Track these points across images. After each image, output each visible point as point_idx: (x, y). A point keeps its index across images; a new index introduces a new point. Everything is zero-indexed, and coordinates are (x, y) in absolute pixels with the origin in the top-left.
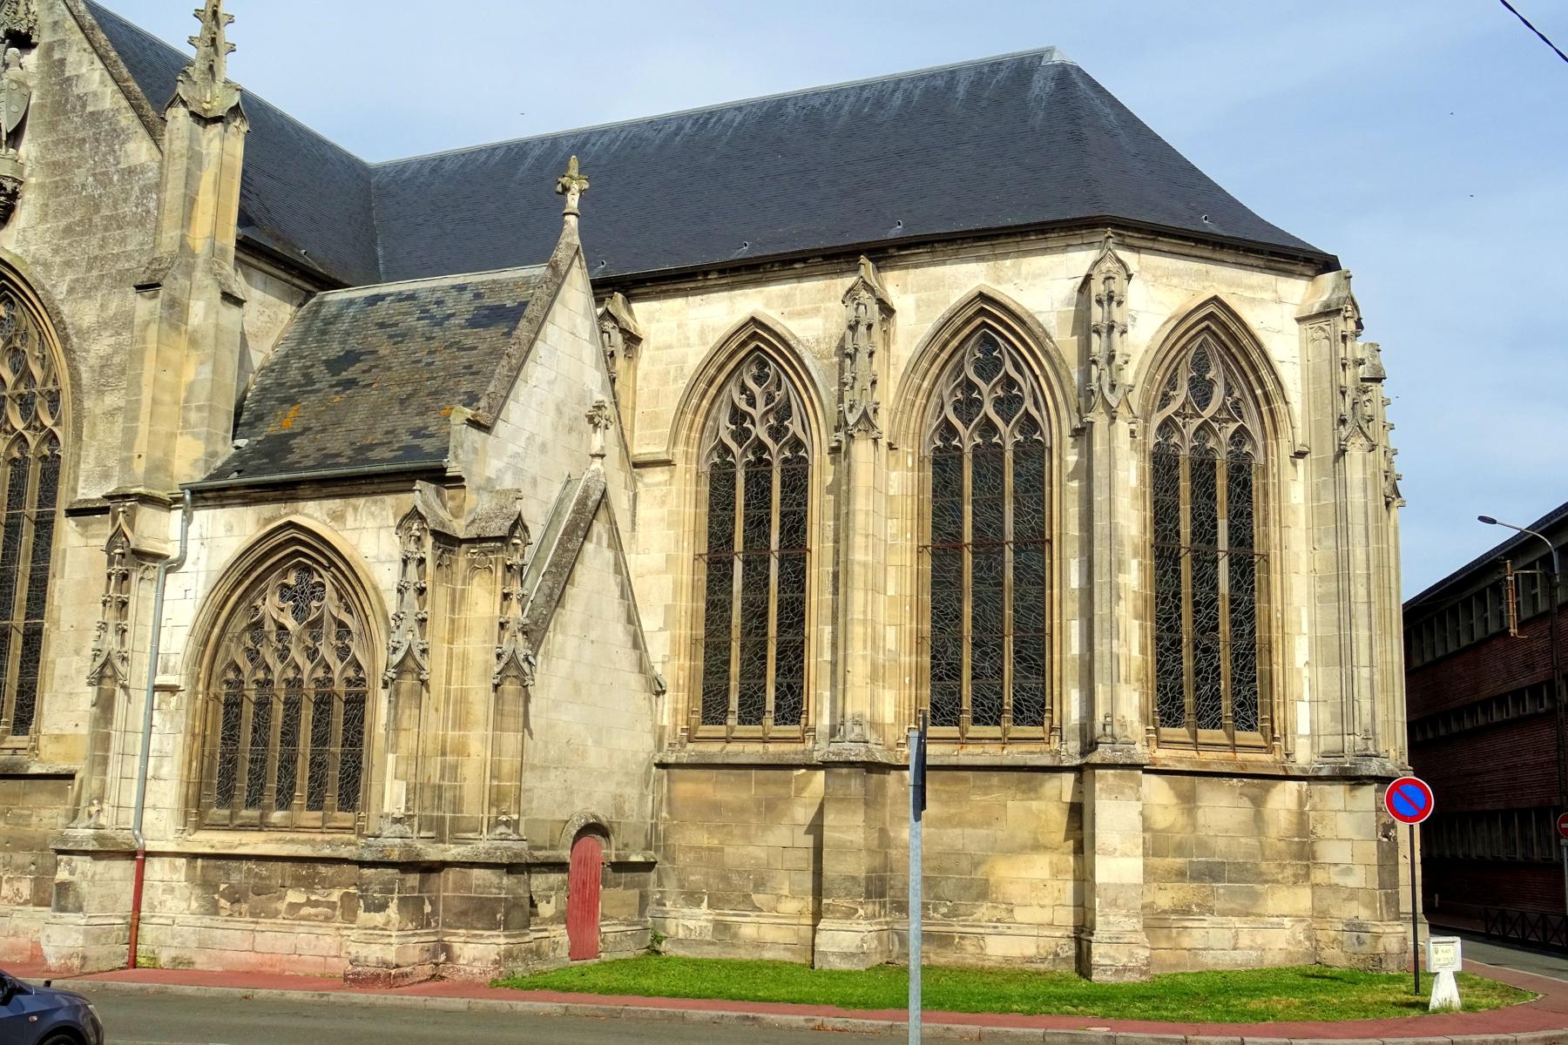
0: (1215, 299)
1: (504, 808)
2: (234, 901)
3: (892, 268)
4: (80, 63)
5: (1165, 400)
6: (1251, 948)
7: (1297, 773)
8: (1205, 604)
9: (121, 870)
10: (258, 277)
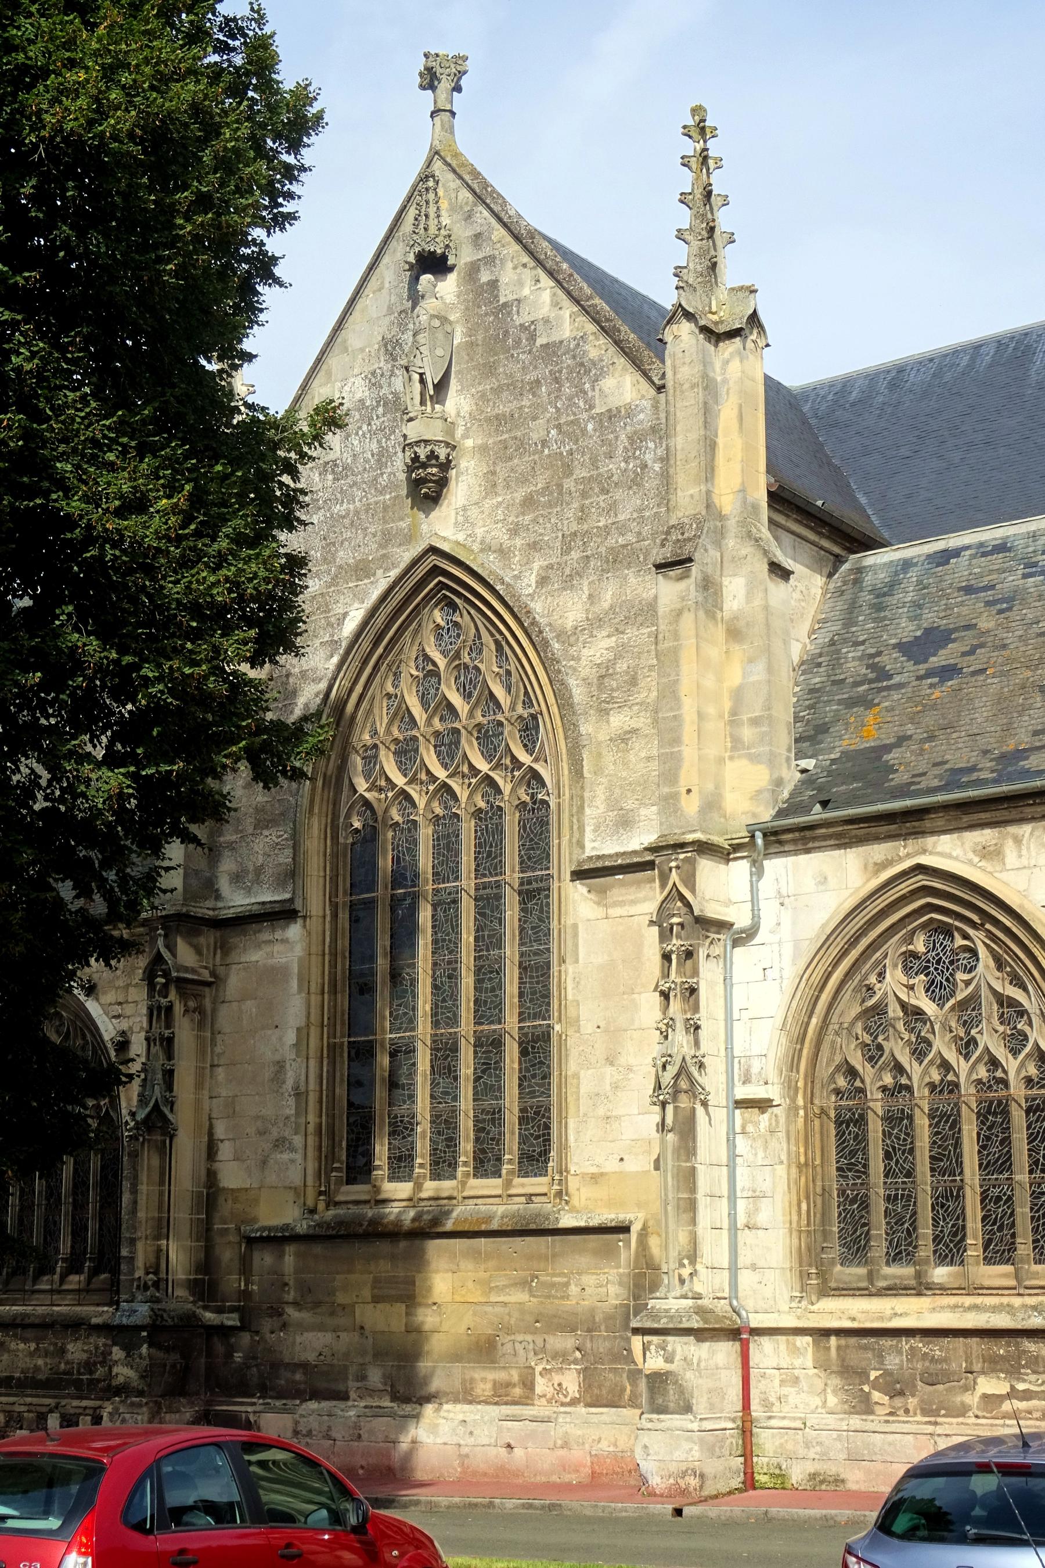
2: (895, 1394)
4: (520, 283)
9: (725, 1352)
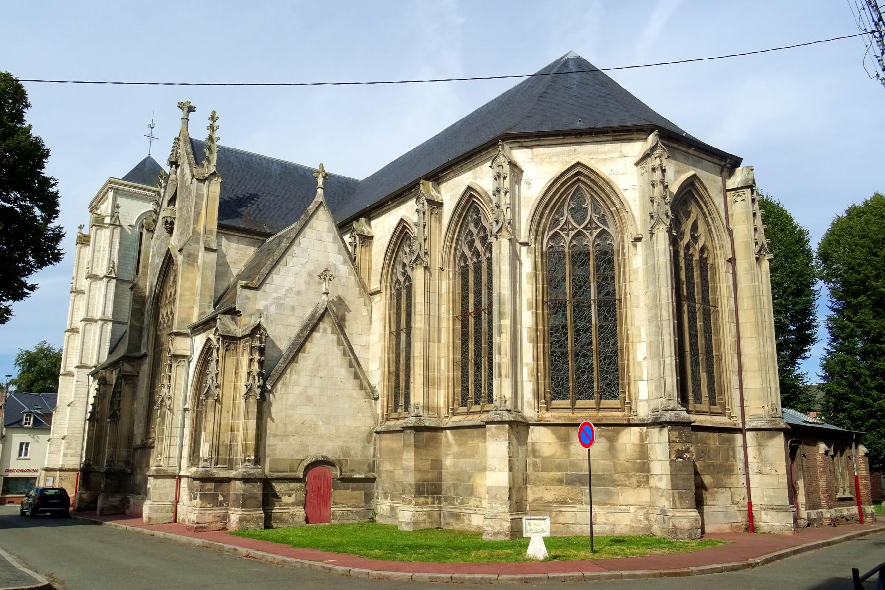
3: (443, 182)
5: (556, 222)
6: (606, 524)
7: (637, 422)
8: (582, 331)
9: (170, 483)
10: (234, 239)
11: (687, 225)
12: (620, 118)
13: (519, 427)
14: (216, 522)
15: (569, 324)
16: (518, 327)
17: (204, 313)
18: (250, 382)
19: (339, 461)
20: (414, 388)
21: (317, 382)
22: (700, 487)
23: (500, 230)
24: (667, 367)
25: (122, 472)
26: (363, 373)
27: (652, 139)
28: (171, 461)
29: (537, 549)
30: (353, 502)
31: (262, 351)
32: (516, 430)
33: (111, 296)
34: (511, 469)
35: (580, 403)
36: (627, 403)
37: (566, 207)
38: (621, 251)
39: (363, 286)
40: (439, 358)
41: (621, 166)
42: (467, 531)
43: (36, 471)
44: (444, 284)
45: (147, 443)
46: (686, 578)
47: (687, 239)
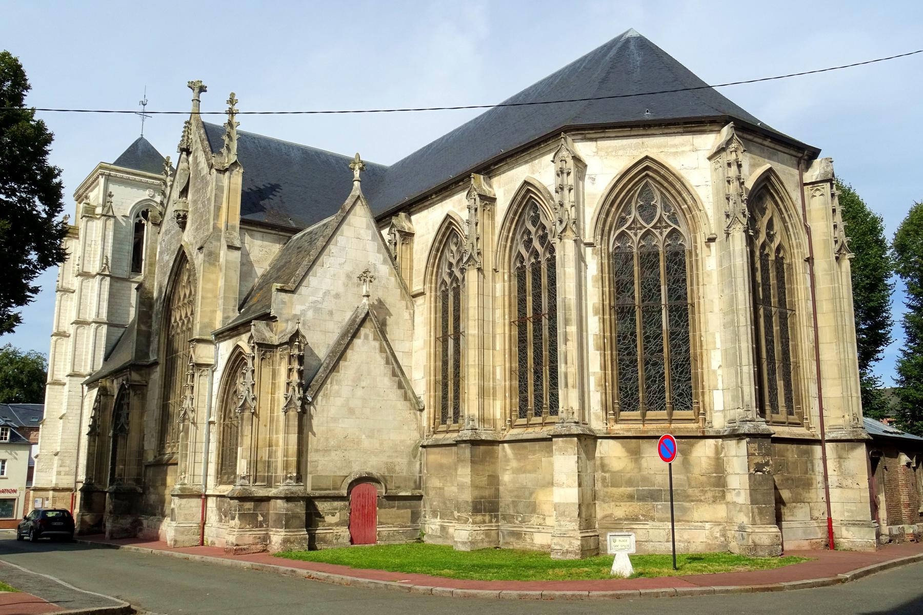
0: (647, 158)
1: (290, 471)
3: (495, 176)
5: (623, 220)
7: (712, 434)
8: (653, 338)
9: (196, 503)
10: (258, 235)
11: (762, 223)
12: (690, 106)
13: (587, 440)
14: (257, 544)
15: (638, 330)
16: (584, 333)
17: (228, 318)
18: (290, 393)
19: (384, 477)
20: (468, 399)
21: (359, 392)
22: (780, 502)
23: (565, 230)
24: (745, 376)
25: (132, 492)
26: (407, 382)
27: (726, 131)
28: (196, 479)
29: (622, 566)
30: (399, 521)
31: (301, 359)
32: (584, 443)
33: (106, 295)
34: (580, 485)
35: (651, 414)
36: (701, 414)
37: (633, 204)
38: (693, 252)
39: (404, 287)
40: (494, 367)
41: (695, 161)
42: (530, 551)
43: (15, 491)
44: (499, 286)
45: (162, 459)
46: (780, 593)
47: (762, 237)
